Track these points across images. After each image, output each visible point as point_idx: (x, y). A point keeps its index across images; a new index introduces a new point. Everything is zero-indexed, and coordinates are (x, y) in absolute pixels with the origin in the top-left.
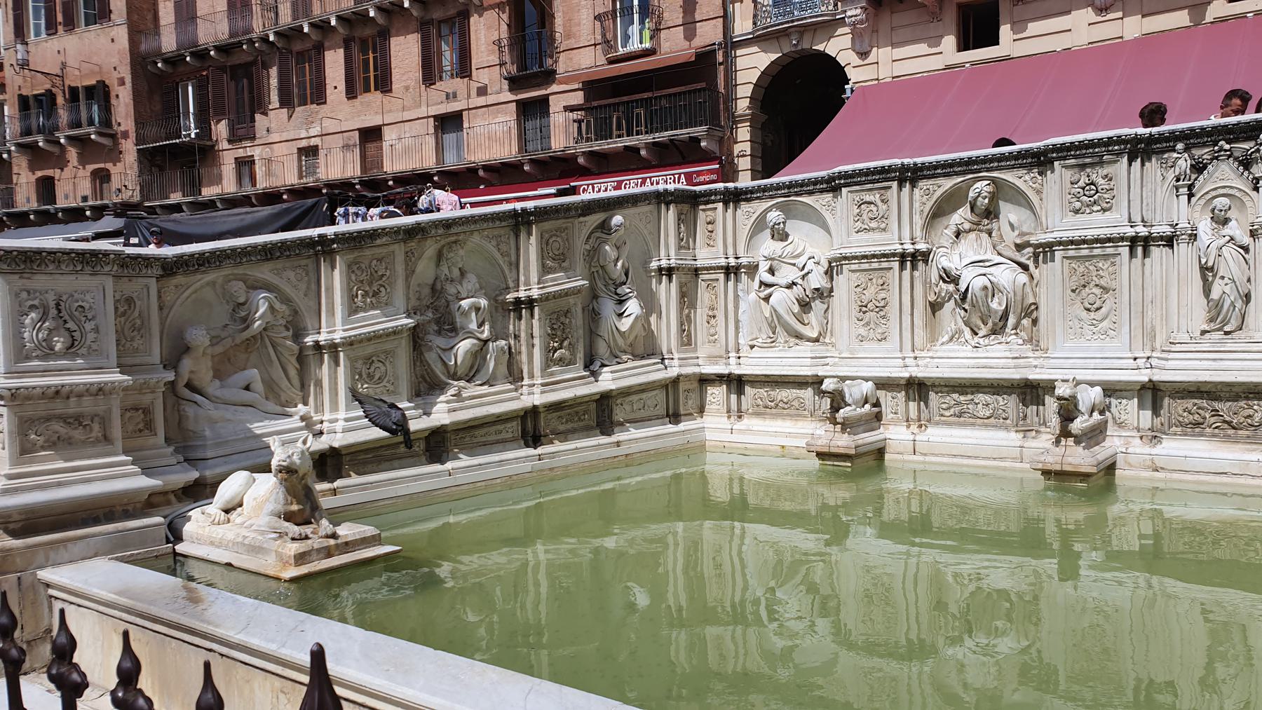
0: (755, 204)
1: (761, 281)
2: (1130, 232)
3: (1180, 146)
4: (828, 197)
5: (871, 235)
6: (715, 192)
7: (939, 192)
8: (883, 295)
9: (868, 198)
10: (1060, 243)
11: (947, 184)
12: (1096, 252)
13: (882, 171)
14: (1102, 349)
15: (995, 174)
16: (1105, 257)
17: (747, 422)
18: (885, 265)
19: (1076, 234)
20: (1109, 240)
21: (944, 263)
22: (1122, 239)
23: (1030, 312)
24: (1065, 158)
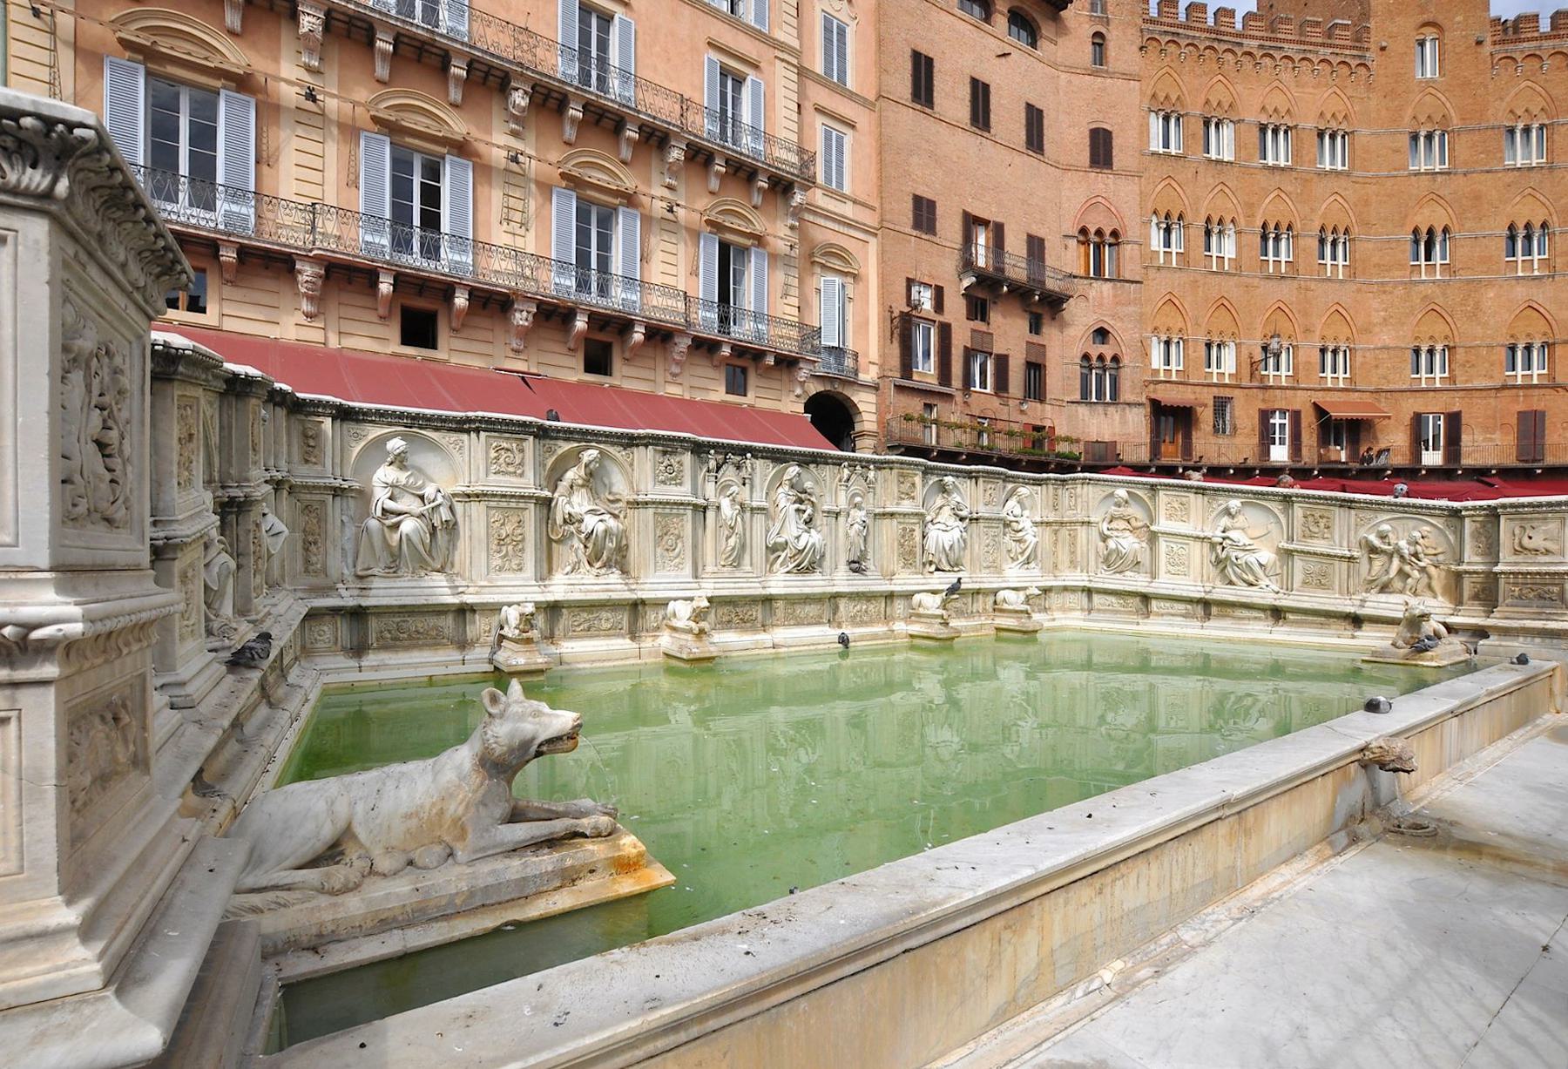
0: (368, 427)
1: (383, 509)
2: (695, 501)
3: (712, 451)
4: (454, 436)
5: (507, 478)
6: (327, 405)
7: (560, 452)
8: (519, 531)
9: (505, 445)
10: (654, 503)
11: (565, 447)
12: (675, 511)
13: (524, 424)
14: (677, 577)
15: (602, 446)
16: (678, 515)
17: (371, 659)
18: (521, 505)
19: (665, 498)
20: (682, 504)
21: (568, 509)
22: (689, 504)
23: (622, 550)
24: (657, 445)
